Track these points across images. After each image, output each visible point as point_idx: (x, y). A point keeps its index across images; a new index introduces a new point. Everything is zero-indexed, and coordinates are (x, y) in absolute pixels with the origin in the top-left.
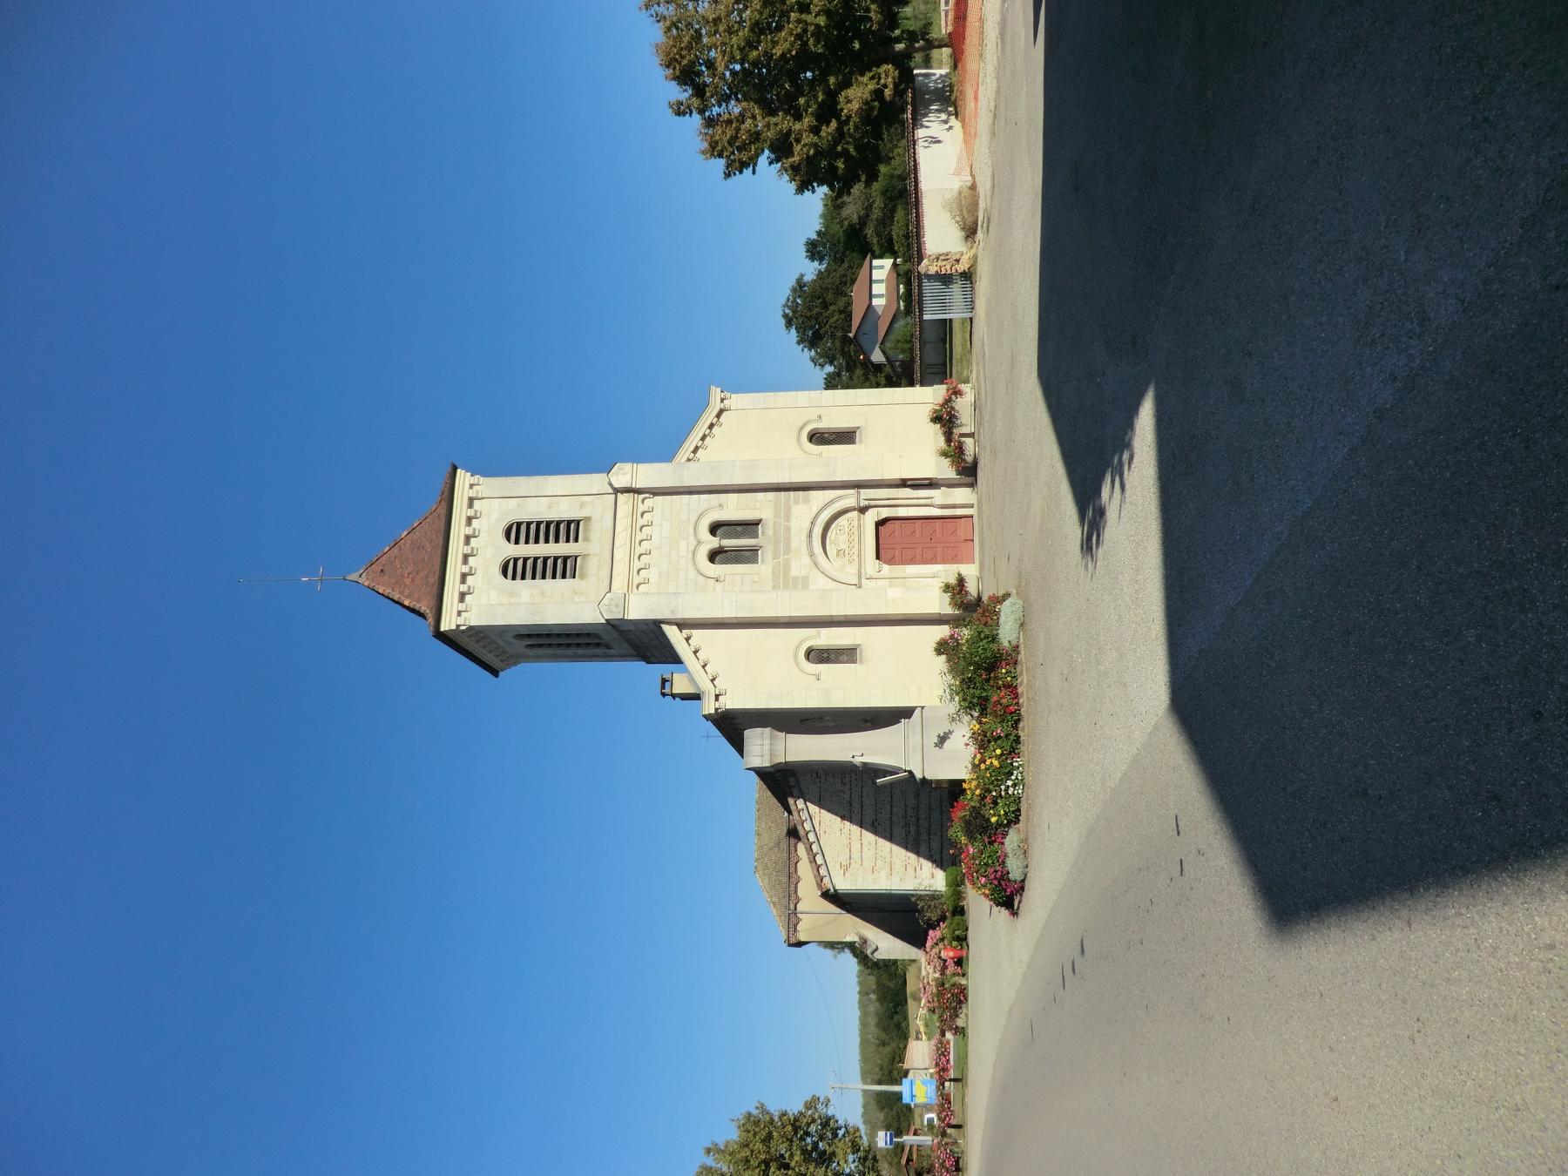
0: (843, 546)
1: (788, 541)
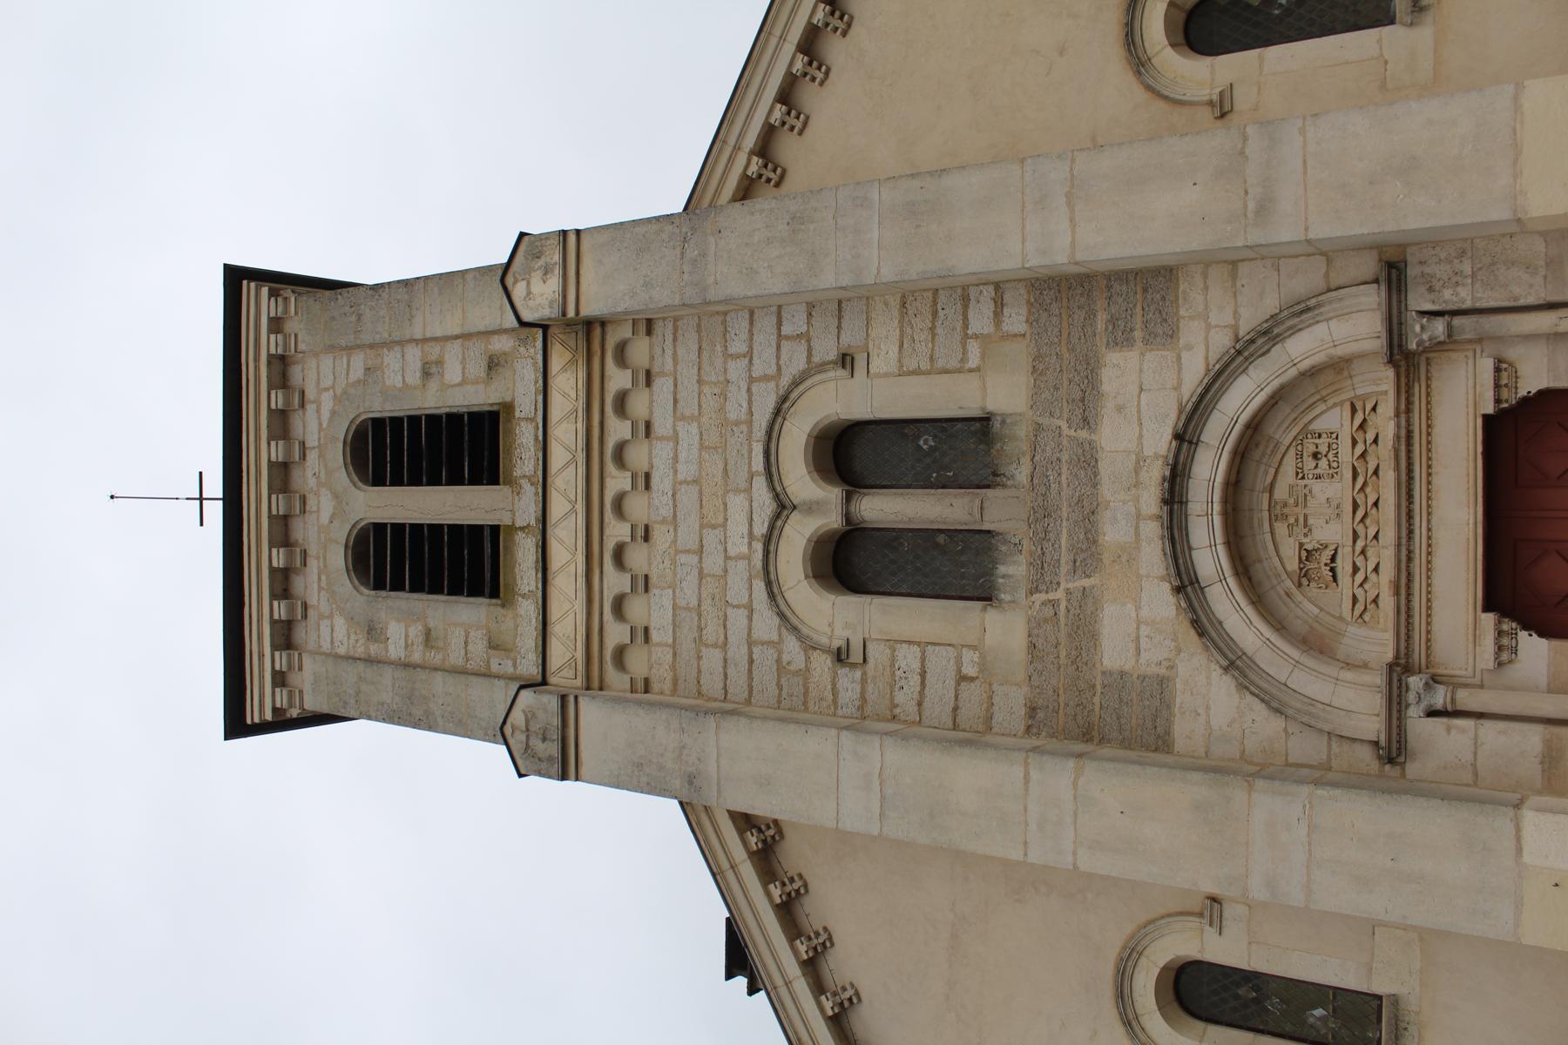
0: (1331, 532)
1: (1089, 515)
